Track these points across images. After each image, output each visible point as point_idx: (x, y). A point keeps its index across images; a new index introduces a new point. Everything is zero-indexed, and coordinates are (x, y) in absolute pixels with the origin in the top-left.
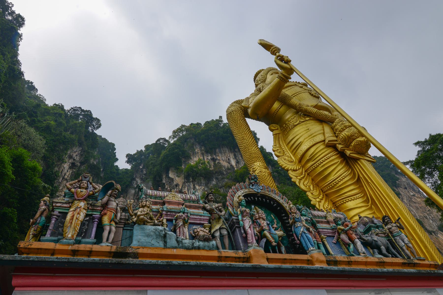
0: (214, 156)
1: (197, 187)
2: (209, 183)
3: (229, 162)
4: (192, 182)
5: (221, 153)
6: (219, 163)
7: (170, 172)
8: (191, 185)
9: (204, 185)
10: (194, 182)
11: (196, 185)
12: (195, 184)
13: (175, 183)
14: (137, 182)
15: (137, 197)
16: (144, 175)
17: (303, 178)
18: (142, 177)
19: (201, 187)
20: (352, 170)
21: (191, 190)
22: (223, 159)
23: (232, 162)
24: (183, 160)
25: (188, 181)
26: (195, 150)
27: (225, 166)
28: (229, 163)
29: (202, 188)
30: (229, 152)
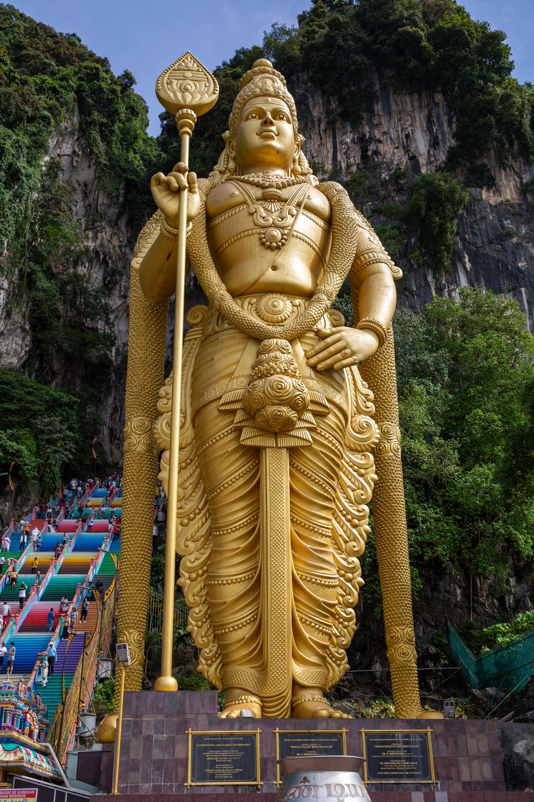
5: (389, 114)
6: (376, 153)
20: (259, 463)
22: (393, 137)
23: (418, 142)
26: (310, 113)
27: (392, 161)
30: (413, 106)
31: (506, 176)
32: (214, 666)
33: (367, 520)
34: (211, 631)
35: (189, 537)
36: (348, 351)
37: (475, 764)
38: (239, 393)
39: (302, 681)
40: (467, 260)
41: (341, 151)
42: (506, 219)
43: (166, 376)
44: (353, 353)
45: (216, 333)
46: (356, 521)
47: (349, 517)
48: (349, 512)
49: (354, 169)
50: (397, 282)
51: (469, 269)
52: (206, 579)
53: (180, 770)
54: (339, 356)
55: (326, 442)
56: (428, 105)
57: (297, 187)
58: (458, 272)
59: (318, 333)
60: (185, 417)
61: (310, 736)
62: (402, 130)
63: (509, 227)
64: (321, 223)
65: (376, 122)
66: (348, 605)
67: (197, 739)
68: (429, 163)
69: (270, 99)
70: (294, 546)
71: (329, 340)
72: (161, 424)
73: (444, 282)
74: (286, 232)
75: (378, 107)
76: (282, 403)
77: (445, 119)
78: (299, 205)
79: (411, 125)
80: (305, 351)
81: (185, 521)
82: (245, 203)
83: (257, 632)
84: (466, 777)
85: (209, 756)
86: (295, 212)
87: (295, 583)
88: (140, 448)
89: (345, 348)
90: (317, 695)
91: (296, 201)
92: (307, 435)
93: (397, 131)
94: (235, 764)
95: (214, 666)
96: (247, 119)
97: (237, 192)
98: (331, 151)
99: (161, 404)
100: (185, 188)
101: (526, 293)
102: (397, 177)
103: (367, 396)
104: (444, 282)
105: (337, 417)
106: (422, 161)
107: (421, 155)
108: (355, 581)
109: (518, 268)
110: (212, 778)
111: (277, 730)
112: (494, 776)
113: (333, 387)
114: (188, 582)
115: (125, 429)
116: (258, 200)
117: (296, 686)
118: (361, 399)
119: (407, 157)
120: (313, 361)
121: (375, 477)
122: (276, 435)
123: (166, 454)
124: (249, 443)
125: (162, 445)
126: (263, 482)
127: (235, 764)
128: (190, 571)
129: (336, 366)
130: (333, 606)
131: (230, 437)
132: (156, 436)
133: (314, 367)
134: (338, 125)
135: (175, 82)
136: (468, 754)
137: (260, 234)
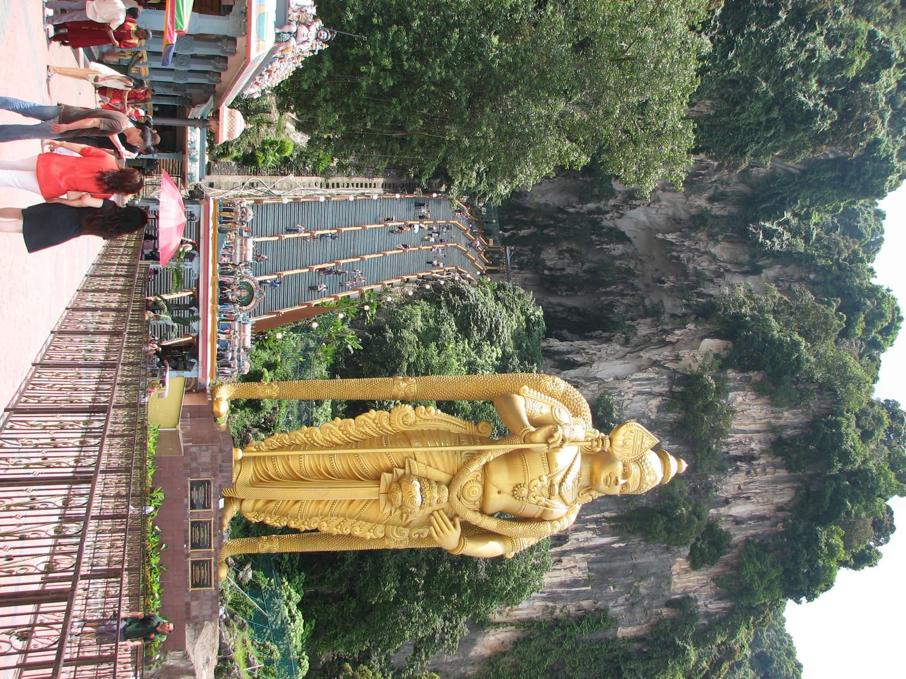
0: (762, 461)
2: (664, 431)
3: (741, 496)
4: (671, 393)
5: (775, 482)
6: (737, 470)
7: (717, 342)
13: (685, 353)
14: (769, 267)
15: (722, 270)
16: (787, 284)
18: (782, 281)
19: (655, 410)
24: (755, 376)
25: (672, 381)
26: (787, 411)
27: (726, 484)
28: (736, 497)
29: (650, 414)
30: (777, 503)
31: (698, 580)
40: (621, 545)
41: (744, 437)
49: (725, 449)
52: (306, 444)
53: (195, 475)
54: (438, 529)
56: (776, 517)
62: (756, 493)
64: (537, 515)
65: (768, 470)
67: (209, 482)
68: (719, 516)
71: (450, 524)
75: (782, 473)
77: (760, 531)
78: (547, 506)
79: (758, 502)
80: (443, 509)
88: (395, 390)
92: (387, 510)
93: (756, 489)
98: (747, 428)
102: (708, 488)
106: (723, 510)
107: (730, 508)
110: (192, 489)
117: (242, 500)
119: (729, 496)
120: (436, 513)
131: (389, 464)
133: (432, 514)
134: (771, 436)
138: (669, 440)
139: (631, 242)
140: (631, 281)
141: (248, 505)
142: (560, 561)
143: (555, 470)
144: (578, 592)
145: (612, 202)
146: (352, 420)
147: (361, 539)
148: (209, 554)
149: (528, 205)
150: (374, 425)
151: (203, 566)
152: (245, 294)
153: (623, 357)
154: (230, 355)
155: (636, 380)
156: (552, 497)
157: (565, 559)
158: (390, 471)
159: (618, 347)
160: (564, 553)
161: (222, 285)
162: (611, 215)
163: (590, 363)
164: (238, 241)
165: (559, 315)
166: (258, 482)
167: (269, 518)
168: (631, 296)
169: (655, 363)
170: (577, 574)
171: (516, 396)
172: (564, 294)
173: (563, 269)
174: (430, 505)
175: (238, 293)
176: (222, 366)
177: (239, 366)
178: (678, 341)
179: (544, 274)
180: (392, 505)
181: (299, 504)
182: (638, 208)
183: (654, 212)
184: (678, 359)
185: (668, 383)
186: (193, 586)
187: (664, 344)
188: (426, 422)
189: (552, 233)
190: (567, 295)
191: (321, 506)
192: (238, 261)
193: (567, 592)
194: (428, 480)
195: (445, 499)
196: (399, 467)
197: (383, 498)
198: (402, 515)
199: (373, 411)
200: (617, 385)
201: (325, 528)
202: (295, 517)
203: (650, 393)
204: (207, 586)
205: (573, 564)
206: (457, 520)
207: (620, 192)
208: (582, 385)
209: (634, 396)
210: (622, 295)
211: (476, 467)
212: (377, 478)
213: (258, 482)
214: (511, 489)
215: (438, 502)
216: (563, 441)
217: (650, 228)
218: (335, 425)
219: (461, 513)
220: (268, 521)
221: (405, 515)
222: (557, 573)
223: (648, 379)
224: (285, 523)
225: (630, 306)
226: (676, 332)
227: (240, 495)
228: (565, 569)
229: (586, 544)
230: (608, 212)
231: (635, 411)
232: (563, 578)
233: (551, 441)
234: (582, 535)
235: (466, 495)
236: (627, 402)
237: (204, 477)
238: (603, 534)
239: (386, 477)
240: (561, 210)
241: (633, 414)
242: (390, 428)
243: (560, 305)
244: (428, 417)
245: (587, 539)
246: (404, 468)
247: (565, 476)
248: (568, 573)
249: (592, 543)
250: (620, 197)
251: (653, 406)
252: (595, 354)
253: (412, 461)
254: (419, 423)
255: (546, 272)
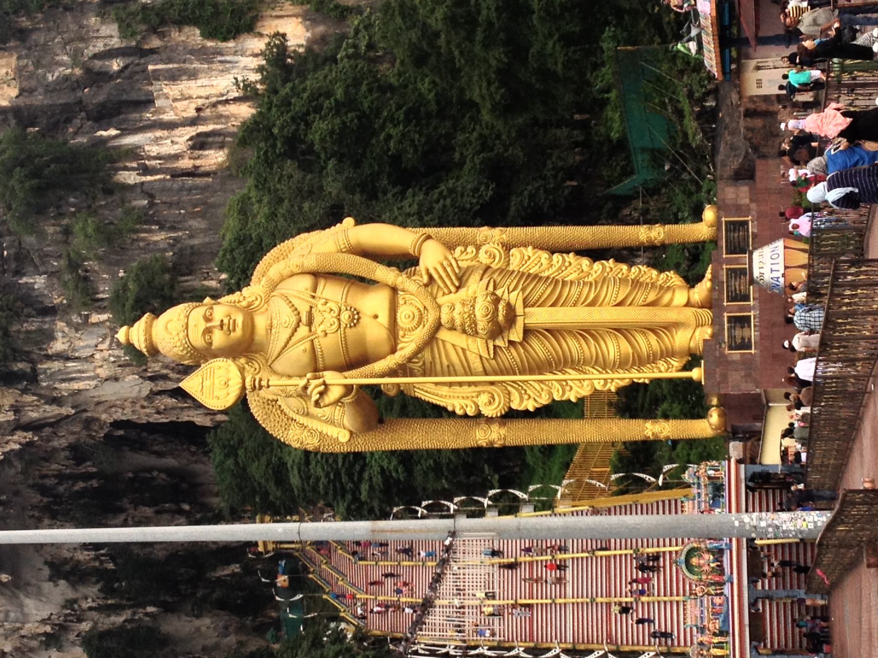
1: (59, 346)
2: (42, 303)
8: (50, 369)
9: (47, 319)
10: (35, 356)
11: (50, 352)
12: (43, 353)
17: (525, 391)
21: (69, 370)
25: (33, 378)
29: (66, 329)
32: (672, 362)
33: (564, 255)
34: (649, 366)
35: (579, 385)
36: (445, 263)
37: (742, 195)
38: (480, 343)
39: (684, 301)
42: (44, 76)
43: (445, 409)
44: (446, 258)
45: (424, 363)
46: (567, 264)
47: (563, 268)
48: (560, 268)
50: (359, 222)
51: (118, 132)
53: (747, 356)
54: (449, 269)
55: (515, 282)
57: (291, 299)
58: (121, 146)
59: (426, 285)
60: (484, 392)
61: (727, 286)
63: (58, 77)
64: (322, 282)
66: (629, 270)
67: (730, 348)
69: (191, 324)
70: (593, 304)
71: (436, 276)
72: (488, 411)
73: (134, 165)
74: (343, 308)
76: (497, 309)
78: (313, 297)
80: (444, 294)
81: (568, 388)
82: (312, 341)
83: (653, 331)
84: (747, 201)
85: (739, 341)
86: (323, 301)
87: (619, 304)
88: (503, 431)
89: (442, 265)
90: (692, 291)
91: (311, 300)
94: (742, 327)
95: (672, 362)
96: (211, 344)
97: (302, 348)
99: (471, 412)
100: (324, 381)
101: (156, 64)
103: (462, 252)
104: (134, 165)
105: (494, 273)
108: (612, 266)
109: (121, 71)
110: (750, 339)
111: (725, 304)
112: (746, 184)
113: (470, 275)
114: (614, 383)
115: (485, 445)
116: (310, 331)
117: (688, 304)
118: (464, 257)
120: (453, 289)
121: (530, 248)
122: (515, 316)
123: (515, 406)
124: (521, 335)
125: (506, 410)
126: (548, 326)
127: (742, 327)
128: (605, 384)
129: (457, 271)
130: (633, 281)
131: (513, 350)
132: (499, 415)
133: (458, 288)
135: (215, 394)
136: (736, 199)
137: (345, 328)
138: (34, 289)
139: (46, 563)
140: (46, 500)
141: (680, 297)
142: (198, 110)
143: (307, 345)
144: (170, 61)
145: (85, 626)
146: (557, 398)
147: (539, 246)
148: (729, 261)
149: (222, 613)
150: (529, 392)
151: (735, 248)
152: (694, 561)
153: (98, 403)
154: (710, 488)
155: (88, 378)
156: (308, 309)
157: (192, 113)
158: (511, 343)
159: (104, 417)
160: (192, 122)
161: (720, 570)
162: (85, 605)
163: (153, 394)
164: (706, 623)
165: (161, 439)
166: (670, 327)
167: (654, 276)
168: (46, 476)
169: (56, 401)
170: (172, 90)
171: (354, 431)
172: (155, 473)
173: (158, 512)
174: (463, 304)
175: (702, 562)
176: (718, 478)
177: (698, 478)
178: (12, 433)
179: (190, 504)
180: (508, 305)
181: (619, 300)
182: (39, 618)
183: (12, 615)
184: (16, 409)
185: (37, 375)
186: (746, 223)
187: (35, 427)
188: (464, 395)
189: (183, 570)
190: (150, 470)
191: (592, 296)
192: (705, 599)
193: (184, 62)
194: (464, 332)
195: (445, 311)
196: (500, 347)
197: (519, 310)
198: (495, 288)
199: (531, 409)
200: (119, 370)
201: (585, 262)
202: (623, 281)
203: (68, 359)
204: (731, 223)
205: (178, 104)
206: (425, 279)
207: (73, 643)
208: (173, 369)
209: (92, 356)
210: (61, 477)
211: (407, 348)
212: (528, 332)
213: (670, 327)
214: (361, 320)
215: (452, 308)
216: (305, 388)
217: (18, 587)
218: (578, 392)
219: (422, 289)
220: (654, 273)
221: (491, 288)
222: (204, 92)
223: (72, 379)
224: (633, 269)
225: (46, 460)
226: (17, 447)
227: (690, 311)
228: (190, 98)
229: (159, 133)
230: (91, 609)
231: (91, 333)
232: (192, 83)
233: (323, 387)
234: (167, 148)
235: (417, 313)
236: (104, 346)
237: (736, 354)
238: (134, 153)
239: (516, 335)
240: (168, 608)
241: (96, 329)
242: (509, 388)
243: (160, 455)
244: (463, 402)
245: (157, 140)
246: (495, 346)
247: (293, 334)
248: (187, 92)
249: (150, 135)
250: (72, 637)
251: (60, 340)
252: (143, 407)
253: (485, 354)
254: (474, 395)
255: (186, 507)
